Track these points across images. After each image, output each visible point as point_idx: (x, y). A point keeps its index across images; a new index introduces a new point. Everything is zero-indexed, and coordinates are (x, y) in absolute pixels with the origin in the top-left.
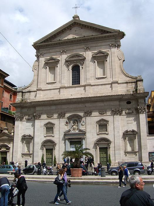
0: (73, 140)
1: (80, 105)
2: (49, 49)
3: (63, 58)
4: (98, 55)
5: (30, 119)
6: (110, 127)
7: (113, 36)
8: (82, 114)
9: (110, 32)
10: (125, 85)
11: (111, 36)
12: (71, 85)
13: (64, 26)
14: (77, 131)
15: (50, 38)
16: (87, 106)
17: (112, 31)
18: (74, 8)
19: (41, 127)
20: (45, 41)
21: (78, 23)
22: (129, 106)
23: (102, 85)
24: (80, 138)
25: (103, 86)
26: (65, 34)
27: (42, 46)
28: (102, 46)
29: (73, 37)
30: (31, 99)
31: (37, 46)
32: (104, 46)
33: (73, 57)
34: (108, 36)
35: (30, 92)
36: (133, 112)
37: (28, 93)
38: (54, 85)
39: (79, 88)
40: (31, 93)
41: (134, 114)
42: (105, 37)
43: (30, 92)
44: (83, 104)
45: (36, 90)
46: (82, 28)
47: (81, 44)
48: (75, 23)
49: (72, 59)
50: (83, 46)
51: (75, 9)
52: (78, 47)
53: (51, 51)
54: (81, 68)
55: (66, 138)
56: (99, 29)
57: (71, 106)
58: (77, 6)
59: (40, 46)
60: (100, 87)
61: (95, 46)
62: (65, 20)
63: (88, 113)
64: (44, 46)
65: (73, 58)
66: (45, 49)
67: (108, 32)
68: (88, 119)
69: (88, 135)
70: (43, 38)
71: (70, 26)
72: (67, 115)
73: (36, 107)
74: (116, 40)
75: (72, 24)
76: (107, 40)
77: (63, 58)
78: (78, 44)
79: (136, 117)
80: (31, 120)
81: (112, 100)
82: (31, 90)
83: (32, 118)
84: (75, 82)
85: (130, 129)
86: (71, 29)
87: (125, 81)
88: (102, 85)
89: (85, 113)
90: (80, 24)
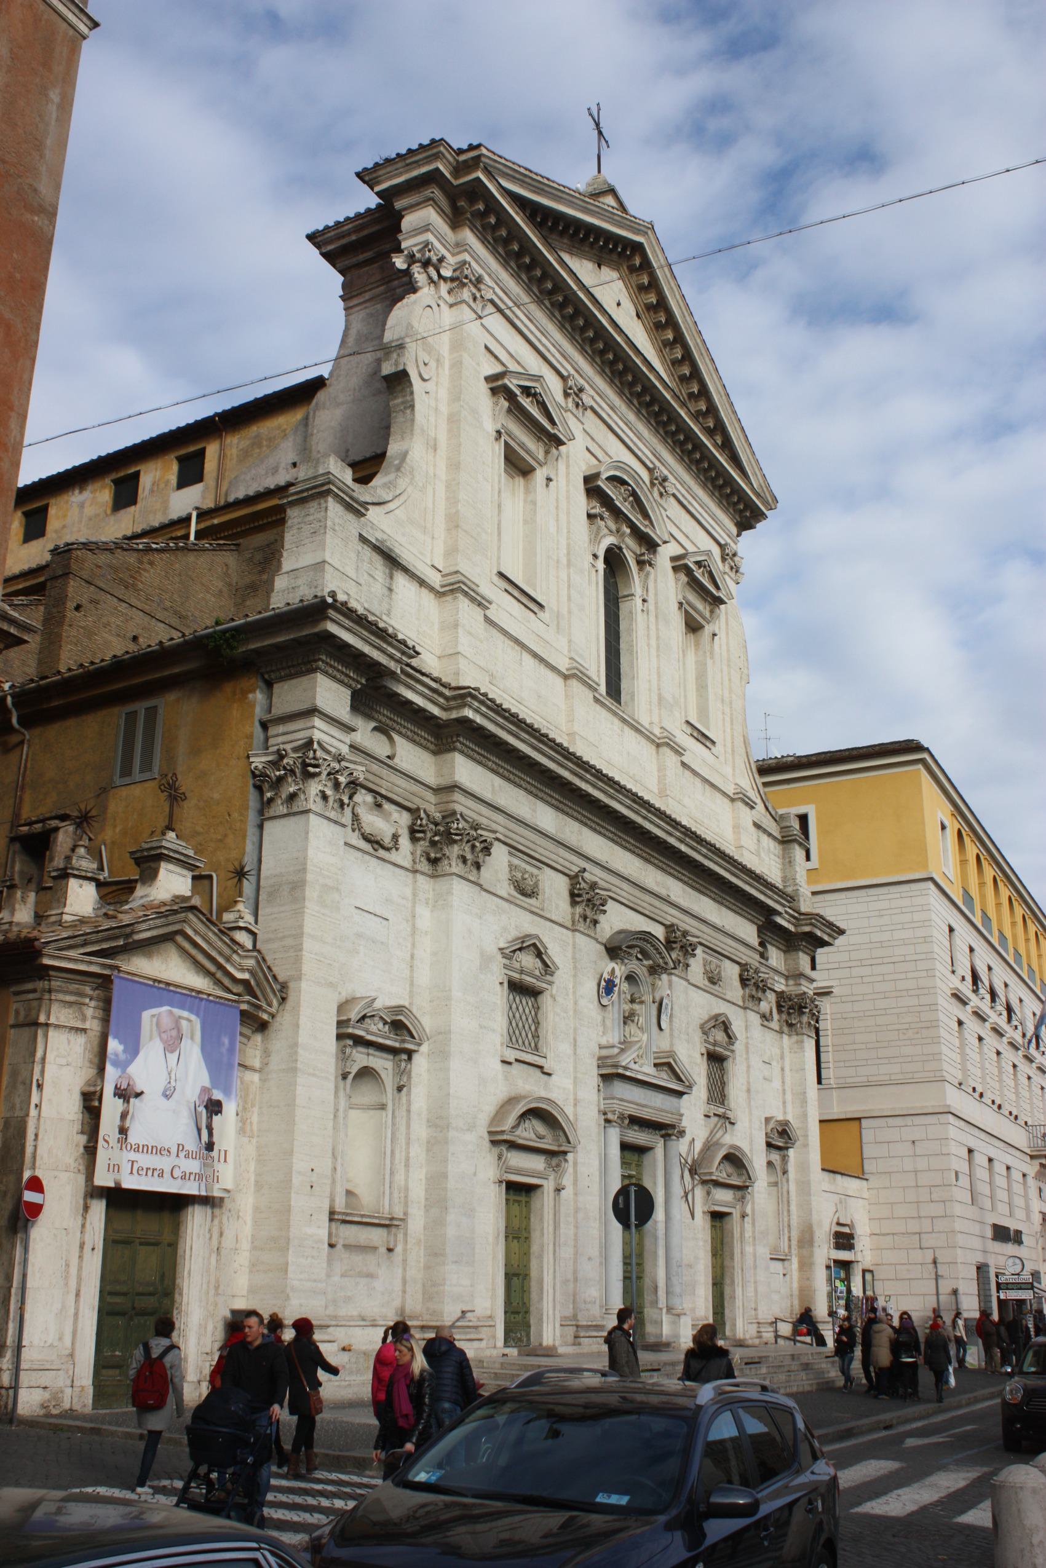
40: (400, 579)
46: (638, 316)
55: (618, 1107)
79: (782, 1048)
80: (393, 856)
90: (654, 285)
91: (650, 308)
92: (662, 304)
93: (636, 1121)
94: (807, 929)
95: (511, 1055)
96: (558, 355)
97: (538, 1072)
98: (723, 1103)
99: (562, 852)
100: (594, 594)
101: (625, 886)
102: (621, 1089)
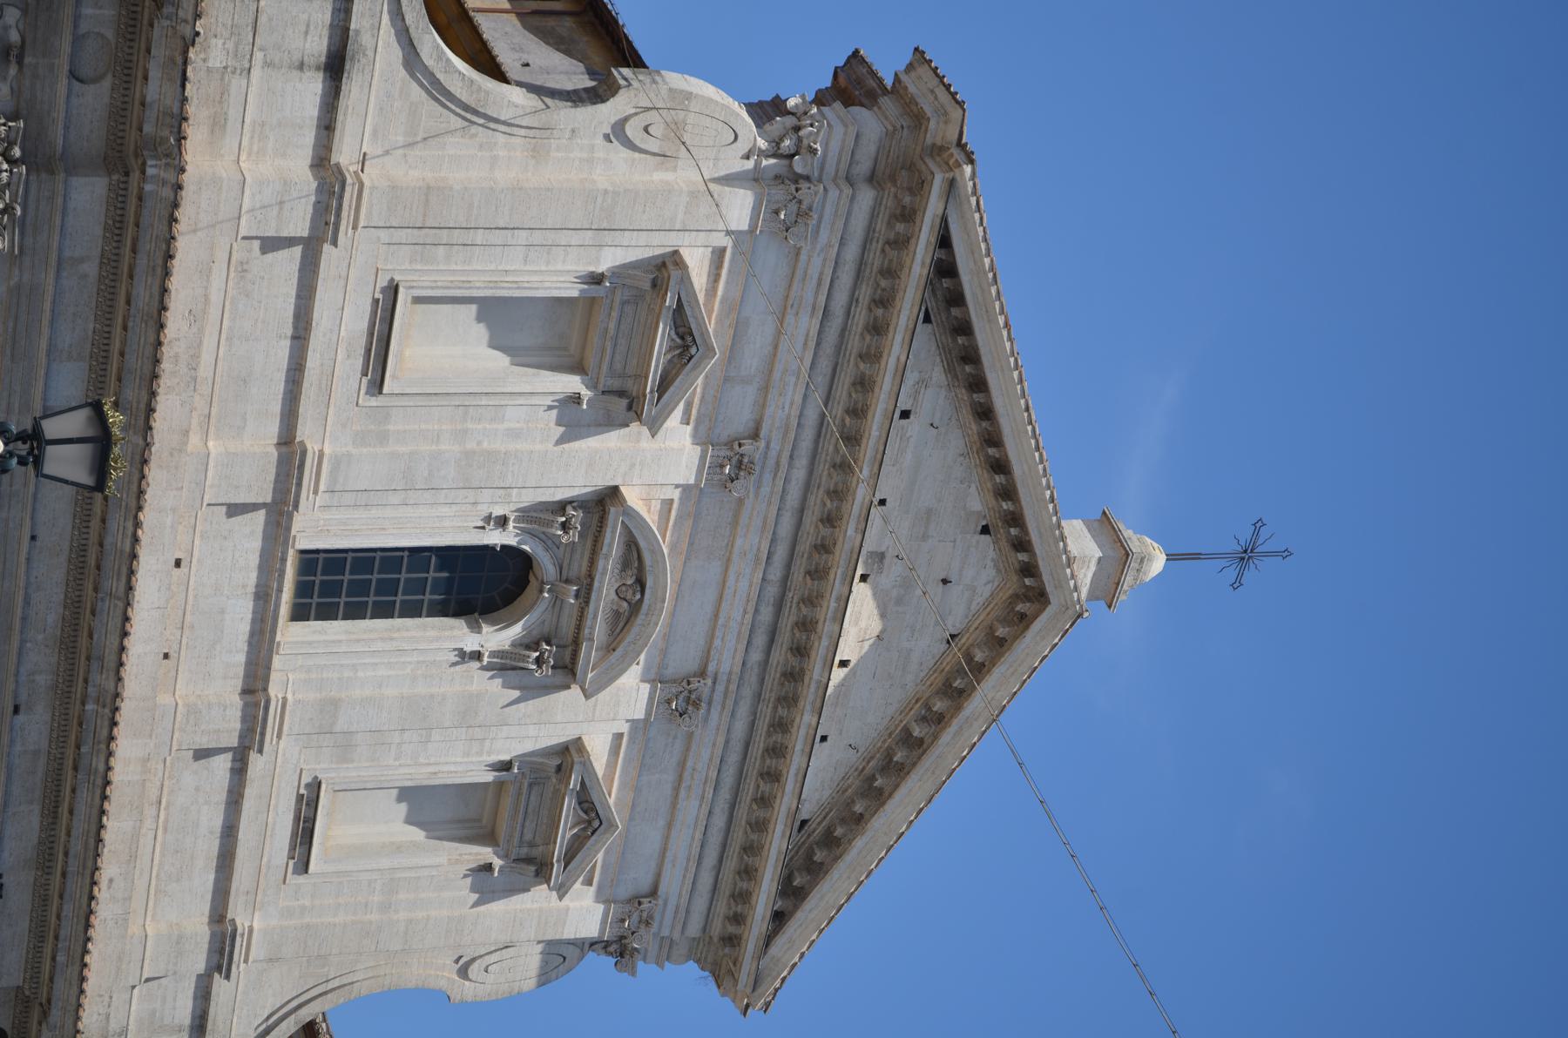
2: (841, 298)
4: (569, 804)
9: (779, 918)
12: (304, 543)
16: (21, 718)
20: (945, 269)
21: (1024, 621)
23: (230, 832)
25: (209, 847)
30: (237, 83)
31: (920, 186)
33: (635, 558)
34: (743, 897)
35: (335, 66)
39: (244, 628)
42: (748, 873)
43: (335, 66)
44: (43, 680)
47: (760, 640)
48: (1039, 597)
50: (727, 658)
52: (736, 613)
53: (804, 325)
56: (858, 821)
59: (908, 215)
60: (213, 819)
61: (682, 765)
65: (625, 565)
66: (852, 252)
67: (792, 893)
75: (1029, 570)
76: (706, 879)
78: (766, 614)
81: (42, 938)
82: (353, 88)
84: (330, 589)
86: (985, 530)
88: (230, 832)
90: (999, 645)
91: (969, 658)
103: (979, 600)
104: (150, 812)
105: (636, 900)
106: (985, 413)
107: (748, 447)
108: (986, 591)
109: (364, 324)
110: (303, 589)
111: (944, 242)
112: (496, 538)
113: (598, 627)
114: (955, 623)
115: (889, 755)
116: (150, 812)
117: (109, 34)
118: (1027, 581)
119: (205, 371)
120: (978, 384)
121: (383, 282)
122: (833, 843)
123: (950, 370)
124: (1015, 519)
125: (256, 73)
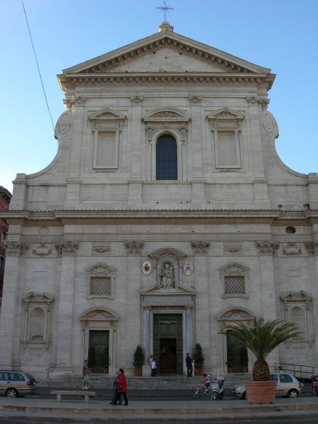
0: (163, 311)
1: (180, 229)
3: (137, 112)
5: (47, 255)
6: (252, 284)
7: (255, 79)
8: (184, 248)
9: (249, 71)
10: (282, 190)
11: (249, 79)
13: (140, 41)
14: (173, 291)
15: (103, 64)
17: (253, 70)
18: (160, 10)
19: (76, 274)
20: (90, 70)
21: (172, 41)
22: (291, 238)
24: (183, 307)
26: (140, 60)
27: (83, 79)
28: (228, 99)
29: (160, 70)
32: (233, 99)
34: (243, 79)
35: (46, 186)
36: (300, 252)
37: (42, 188)
38: (112, 175)
40: (51, 189)
41: (302, 255)
44: (186, 227)
45: (63, 182)
46: (180, 54)
48: (166, 39)
49: (158, 119)
51: (163, 11)
54: (179, 143)
55: (144, 304)
56: (223, 61)
57: (158, 228)
58: (167, 5)
59: (78, 79)
62: (151, 29)
63: (201, 247)
64: (90, 79)
65: (160, 116)
67: (242, 70)
68: (200, 261)
69: (201, 302)
70: (87, 63)
71: (154, 44)
72: (151, 248)
73: (63, 226)
74: (260, 91)
75: (160, 42)
77: (137, 112)
80: (50, 256)
82: (50, 183)
83: (50, 252)
85: (296, 289)
86: (155, 53)
87: (282, 182)
89: (193, 246)
90: (178, 44)
92: (185, 46)
93: (153, 307)
94: (307, 216)
95: (91, 297)
96: (125, 94)
97: (106, 300)
98: (244, 293)
99: (119, 236)
100: (150, 152)
101: (161, 236)
102: (147, 299)
103: (171, 51)
104: (223, 202)
105: (248, 101)
106: (123, 57)
107: (131, 98)
108: (169, 50)
109: (102, 174)
110: (169, 178)
111: (84, 72)
112: (154, 143)
113: (174, 119)
114: (177, 54)
115: (207, 59)
116: (223, 202)
117: (40, 227)
118: (163, 42)
119: (111, 202)
120: (116, 59)
121: (94, 171)
122: (229, 64)
123: (116, 66)
124: (148, 47)
125: (47, 201)
